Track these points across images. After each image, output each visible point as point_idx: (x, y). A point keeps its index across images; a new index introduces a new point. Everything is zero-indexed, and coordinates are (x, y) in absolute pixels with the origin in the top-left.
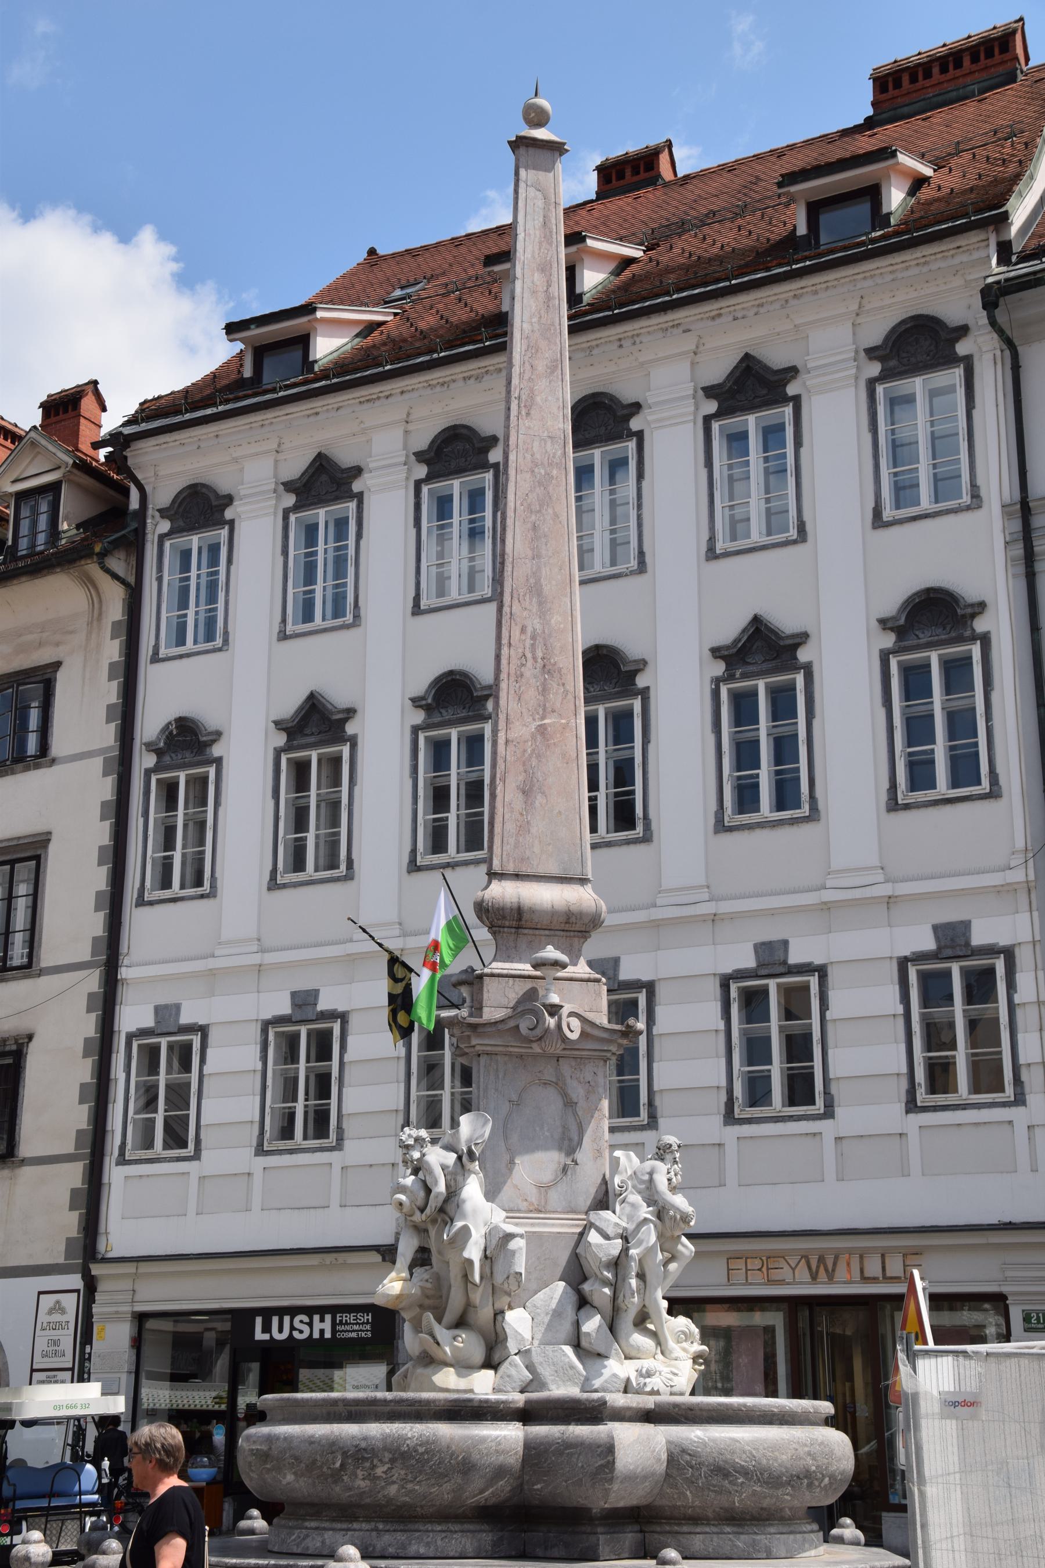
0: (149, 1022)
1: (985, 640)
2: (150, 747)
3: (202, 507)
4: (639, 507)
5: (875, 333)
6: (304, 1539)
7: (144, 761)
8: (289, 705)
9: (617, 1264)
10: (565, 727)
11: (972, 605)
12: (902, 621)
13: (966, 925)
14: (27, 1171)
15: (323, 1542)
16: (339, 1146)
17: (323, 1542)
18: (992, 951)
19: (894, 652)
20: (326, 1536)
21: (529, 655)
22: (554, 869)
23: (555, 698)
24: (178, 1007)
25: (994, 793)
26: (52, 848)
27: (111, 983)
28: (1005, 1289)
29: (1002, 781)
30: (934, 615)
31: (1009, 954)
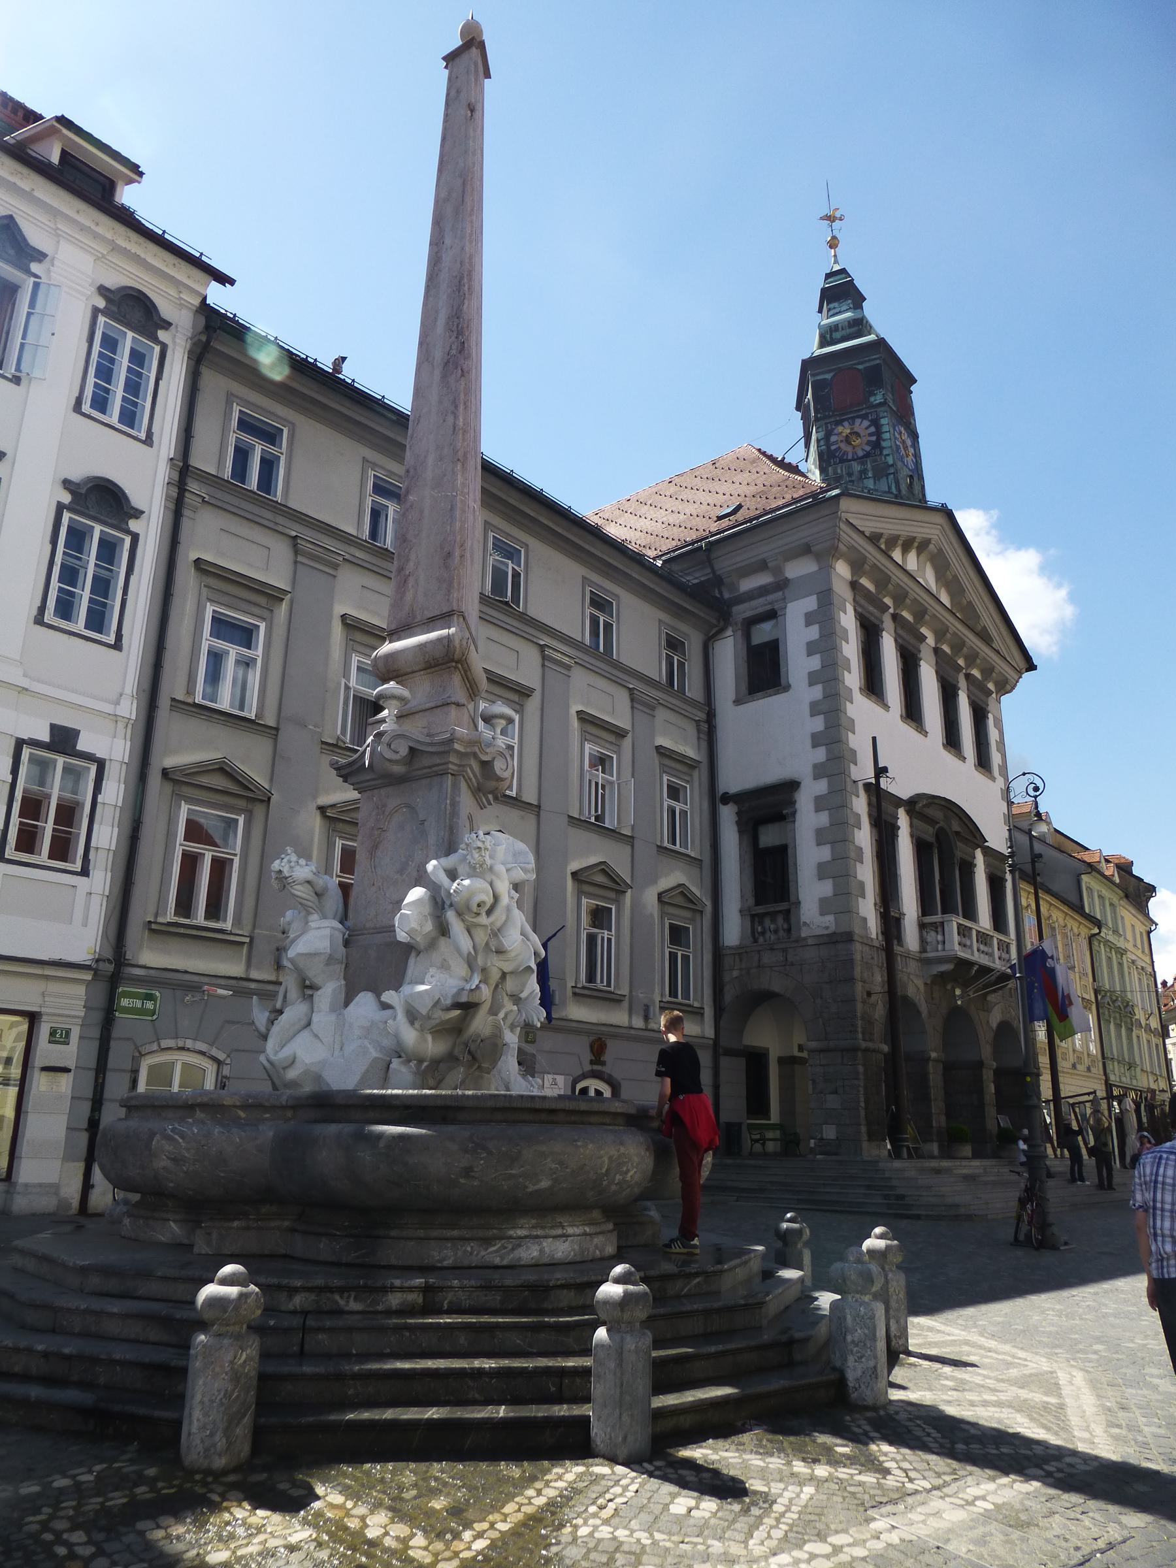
1: (135, 538)
5: (114, 281)
6: (513, 1249)
11: (137, 510)
12: (83, 491)
13: (75, 734)
15: (542, 1251)
17: (542, 1251)
18: (89, 757)
19: (70, 508)
20: (545, 1244)
25: (117, 646)
28: (43, 1010)
29: (125, 641)
30: (101, 499)
31: (101, 764)
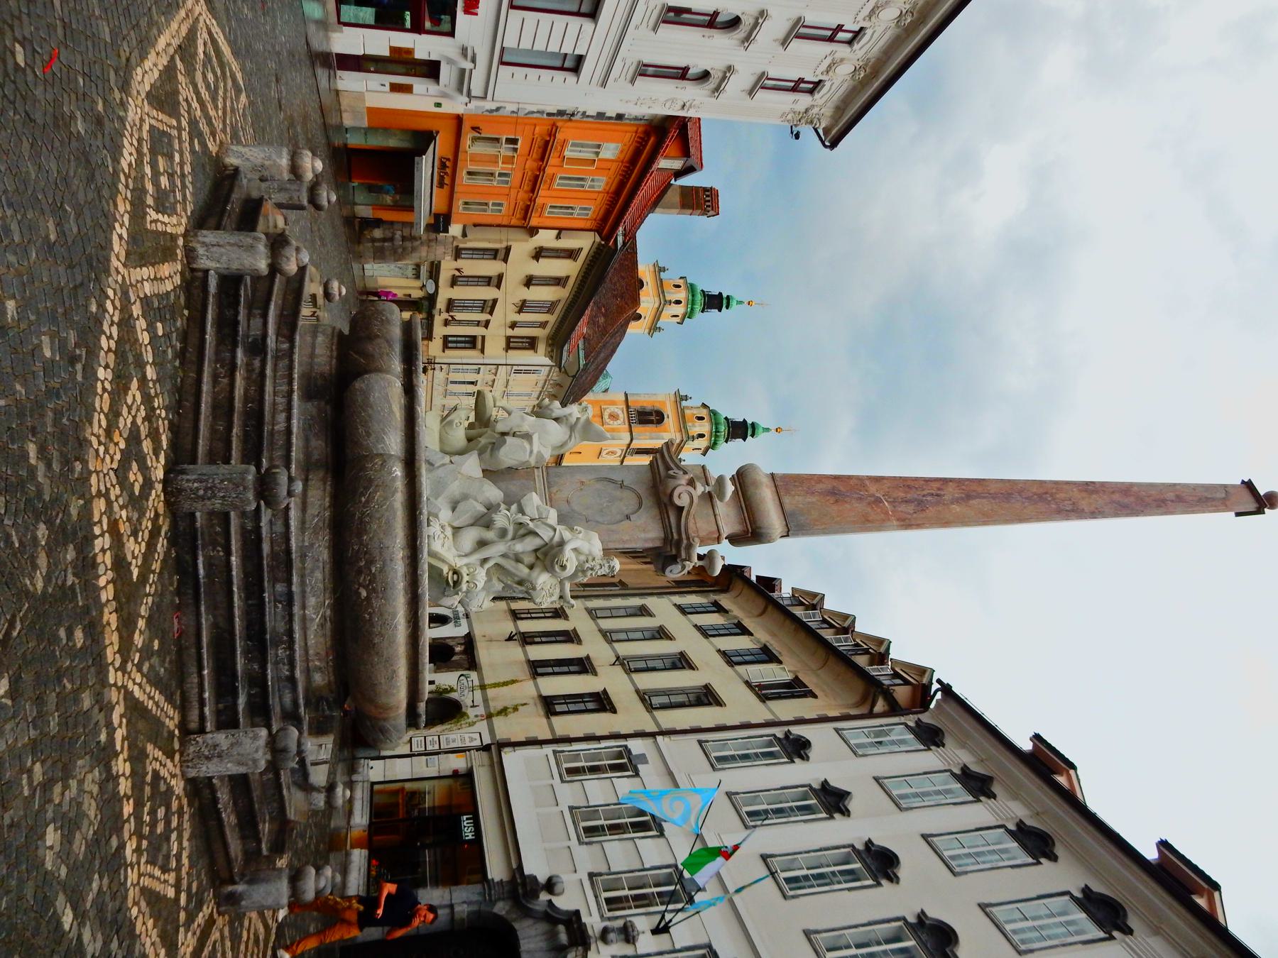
0: (634, 753)
2: (787, 734)
3: (930, 737)
4: (1064, 945)
7: (779, 732)
8: (835, 783)
9: (521, 511)
10: (887, 513)
14: (544, 720)
16: (581, 843)
21: (925, 492)
22: (787, 507)
23: (903, 508)
24: (647, 762)
26: (718, 708)
27: (652, 735)
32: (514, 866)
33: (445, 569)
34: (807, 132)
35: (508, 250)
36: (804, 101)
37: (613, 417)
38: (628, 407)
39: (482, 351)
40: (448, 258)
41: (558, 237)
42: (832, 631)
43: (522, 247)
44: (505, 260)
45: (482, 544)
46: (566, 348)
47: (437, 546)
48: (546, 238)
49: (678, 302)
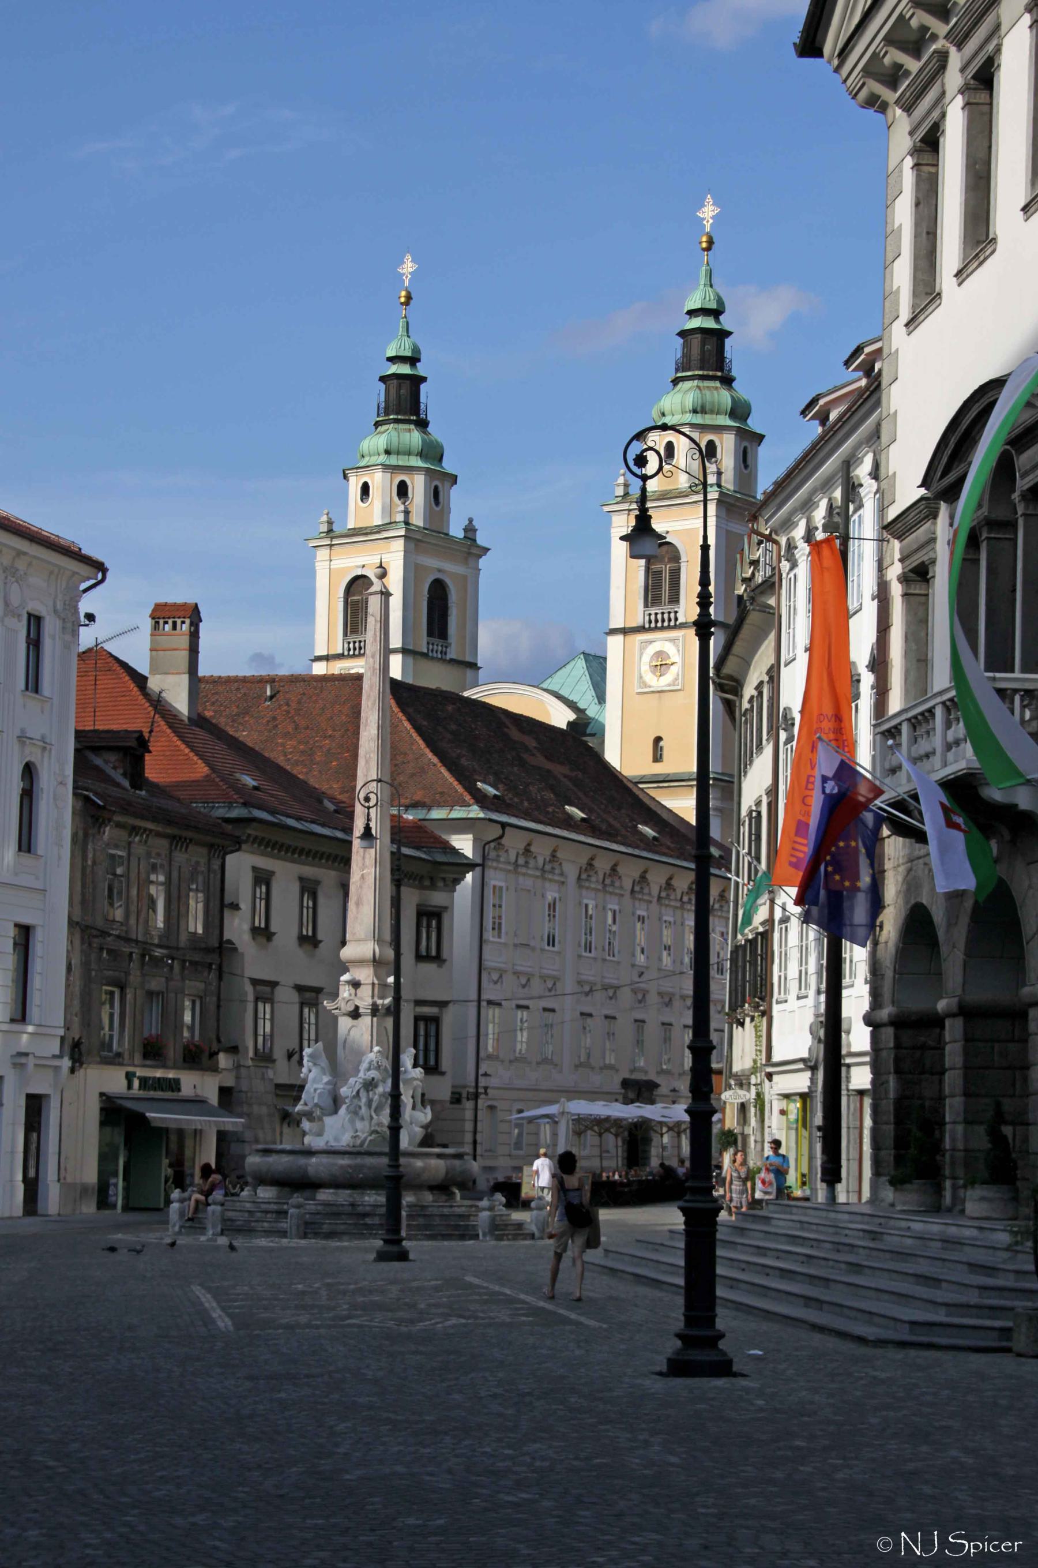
22: (363, 936)
32: (801, 1066)
33: (370, 1138)
34: (85, 605)
35: (255, 982)
36: (51, 627)
37: (661, 665)
38: (640, 629)
39: (443, 1004)
40: (270, 1073)
41: (235, 907)
42: (757, 574)
43: (254, 962)
44: (274, 984)
45: (362, 1119)
46: (440, 858)
47: (358, 1142)
48: (238, 928)
49: (402, 490)
